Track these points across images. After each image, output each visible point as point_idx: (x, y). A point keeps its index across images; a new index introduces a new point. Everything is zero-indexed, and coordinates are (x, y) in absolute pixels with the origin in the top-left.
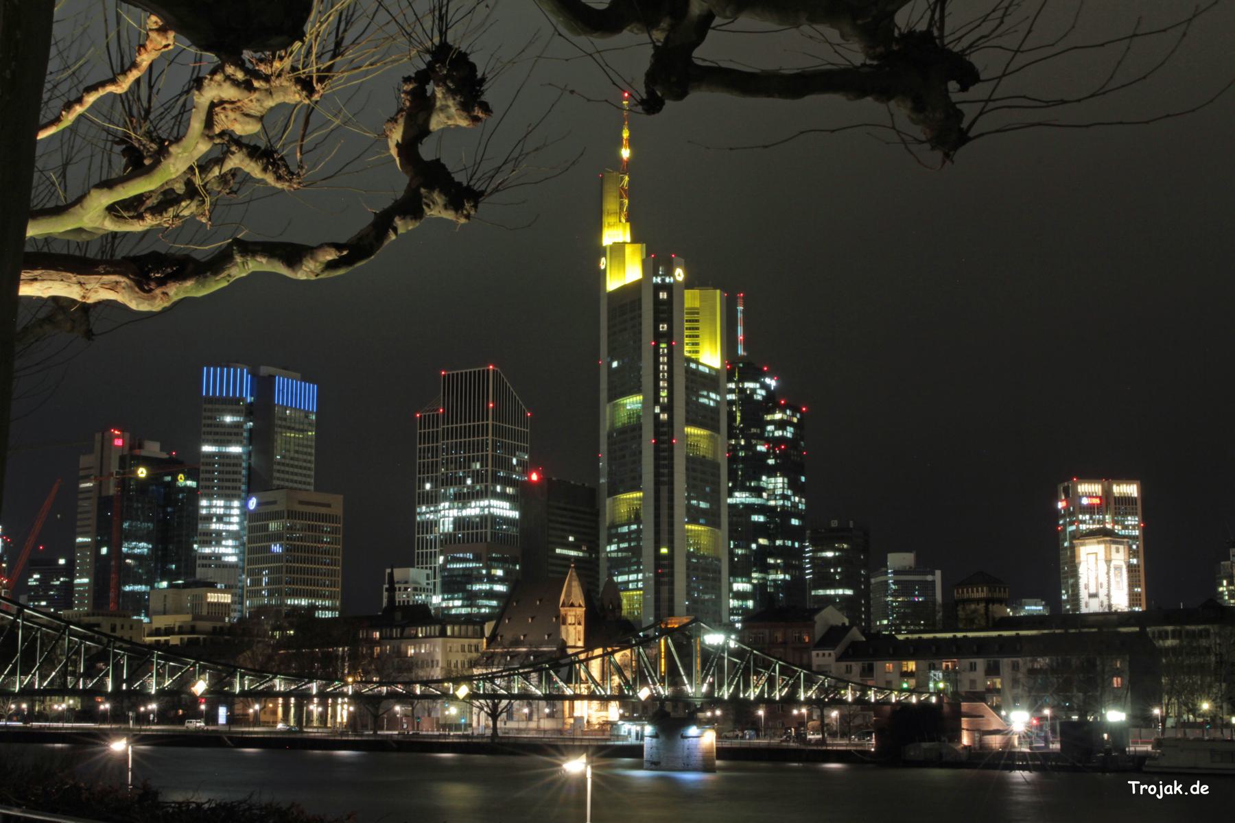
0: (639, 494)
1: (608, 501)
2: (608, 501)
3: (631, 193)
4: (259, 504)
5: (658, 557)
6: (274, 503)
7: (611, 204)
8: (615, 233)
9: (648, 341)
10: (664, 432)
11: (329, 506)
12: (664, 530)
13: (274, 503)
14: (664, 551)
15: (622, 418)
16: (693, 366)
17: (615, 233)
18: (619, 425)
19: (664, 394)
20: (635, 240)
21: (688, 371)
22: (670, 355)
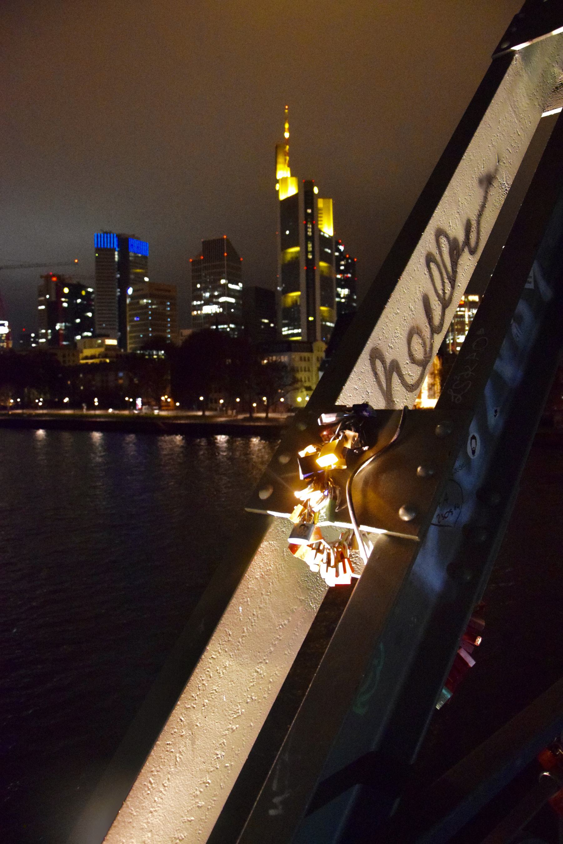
0: (298, 293)
1: (282, 298)
2: (282, 298)
3: (289, 154)
4: (134, 291)
5: (308, 321)
6: (142, 290)
7: (280, 159)
8: (283, 171)
9: (302, 222)
10: (311, 265)
11: (169, 291)
12: (312, 311)
13: (142, 290)
14: (311, 319)
15: (289, 257)
16: (322, 233)
17: (283, 171)
18: (286, 262)
19: (310, 245)
20: (292, 175)
21: (320, 235)
22: (313, 228)
